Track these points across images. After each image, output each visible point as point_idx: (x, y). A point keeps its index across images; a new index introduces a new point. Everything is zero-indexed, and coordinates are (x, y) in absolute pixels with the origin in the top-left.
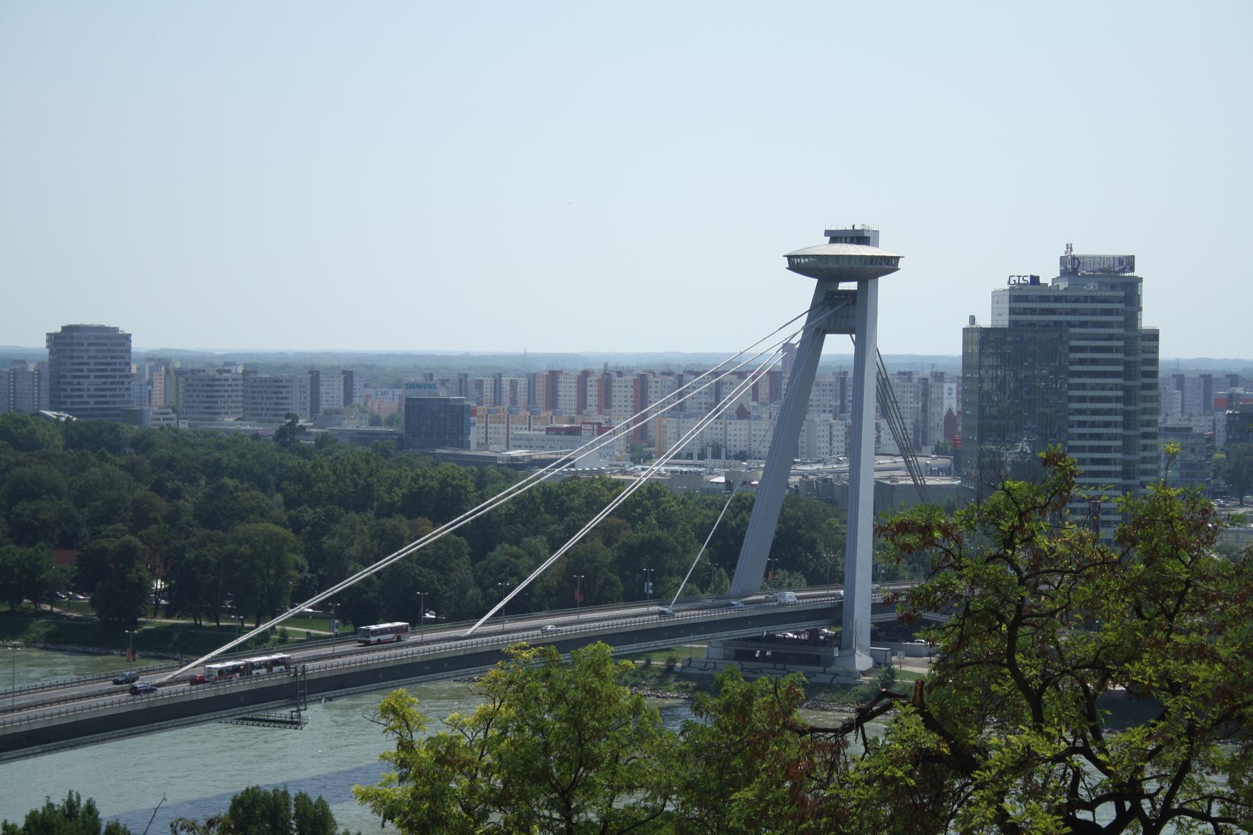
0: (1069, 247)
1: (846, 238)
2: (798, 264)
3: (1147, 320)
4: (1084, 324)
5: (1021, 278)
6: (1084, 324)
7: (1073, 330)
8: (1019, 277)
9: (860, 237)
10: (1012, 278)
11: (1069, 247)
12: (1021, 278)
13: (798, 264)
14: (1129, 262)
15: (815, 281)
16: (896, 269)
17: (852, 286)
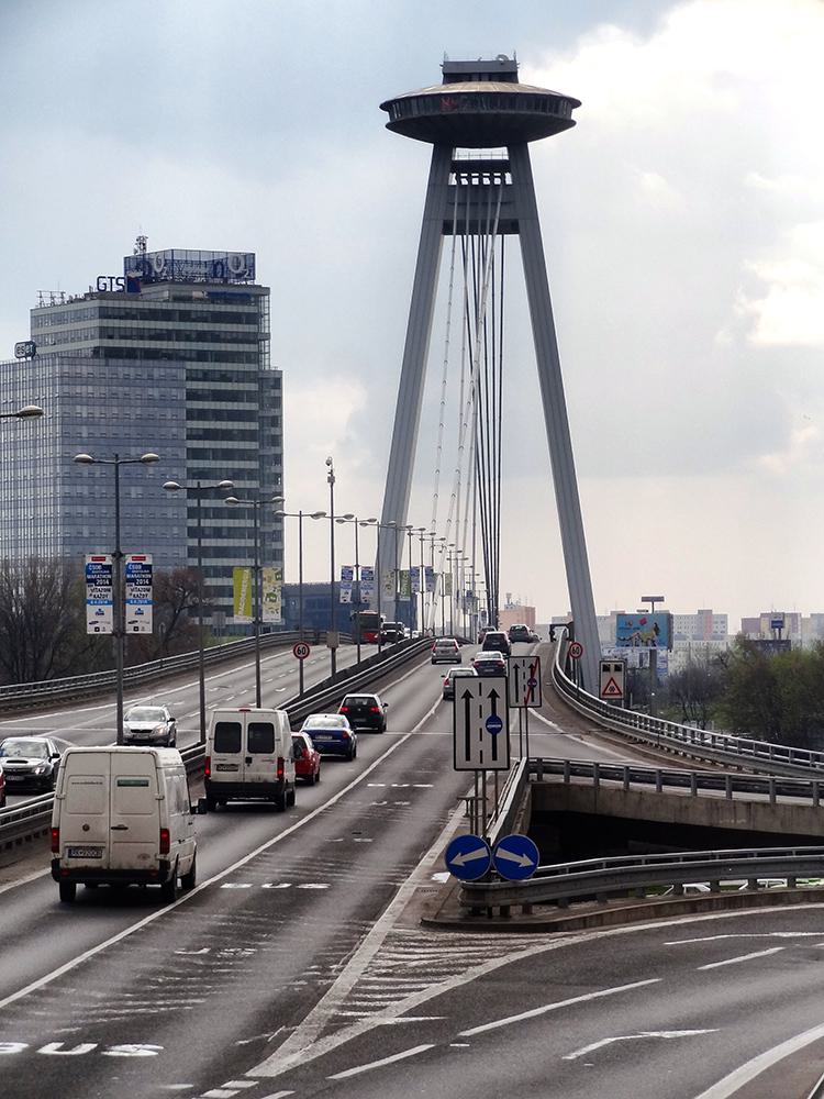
0: (142, 242)
1: (480, 74)
2: (408, 116)
3: (278, 356)
4: (202, 356)
5: (114, 281)
6: (202, 356)
7: (189, 365)
8: (111, 278)
9: (507, 72)
10: (104, 281)
11: (142, 242)
12: (114, 281)
13: (408, 116)
14: (247, 263)
15: (432, 145)
16: (572, 123)
17: (500, 153)
